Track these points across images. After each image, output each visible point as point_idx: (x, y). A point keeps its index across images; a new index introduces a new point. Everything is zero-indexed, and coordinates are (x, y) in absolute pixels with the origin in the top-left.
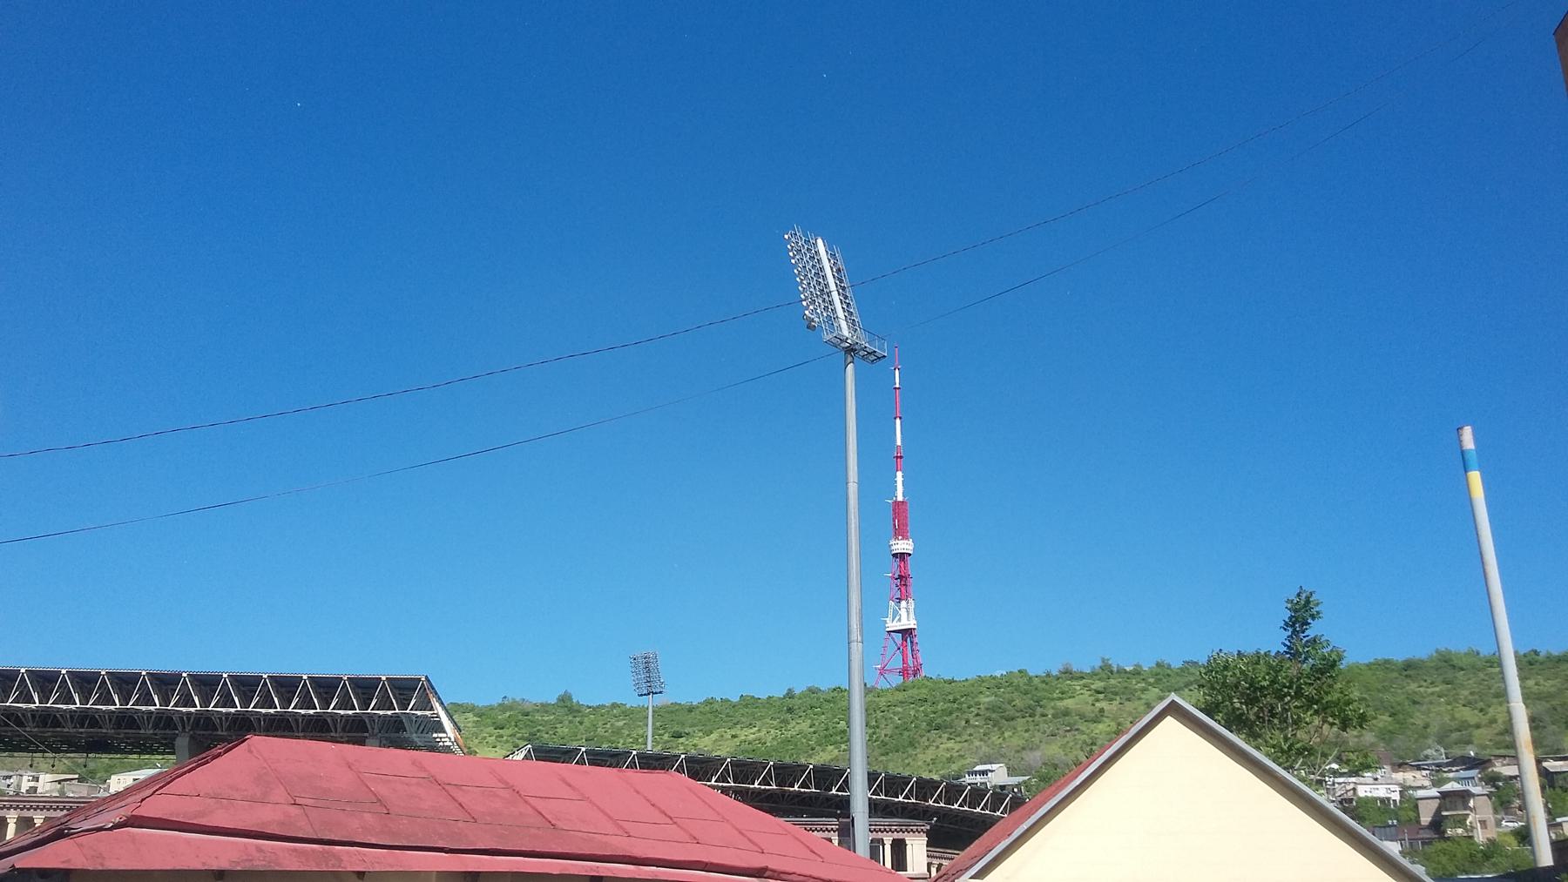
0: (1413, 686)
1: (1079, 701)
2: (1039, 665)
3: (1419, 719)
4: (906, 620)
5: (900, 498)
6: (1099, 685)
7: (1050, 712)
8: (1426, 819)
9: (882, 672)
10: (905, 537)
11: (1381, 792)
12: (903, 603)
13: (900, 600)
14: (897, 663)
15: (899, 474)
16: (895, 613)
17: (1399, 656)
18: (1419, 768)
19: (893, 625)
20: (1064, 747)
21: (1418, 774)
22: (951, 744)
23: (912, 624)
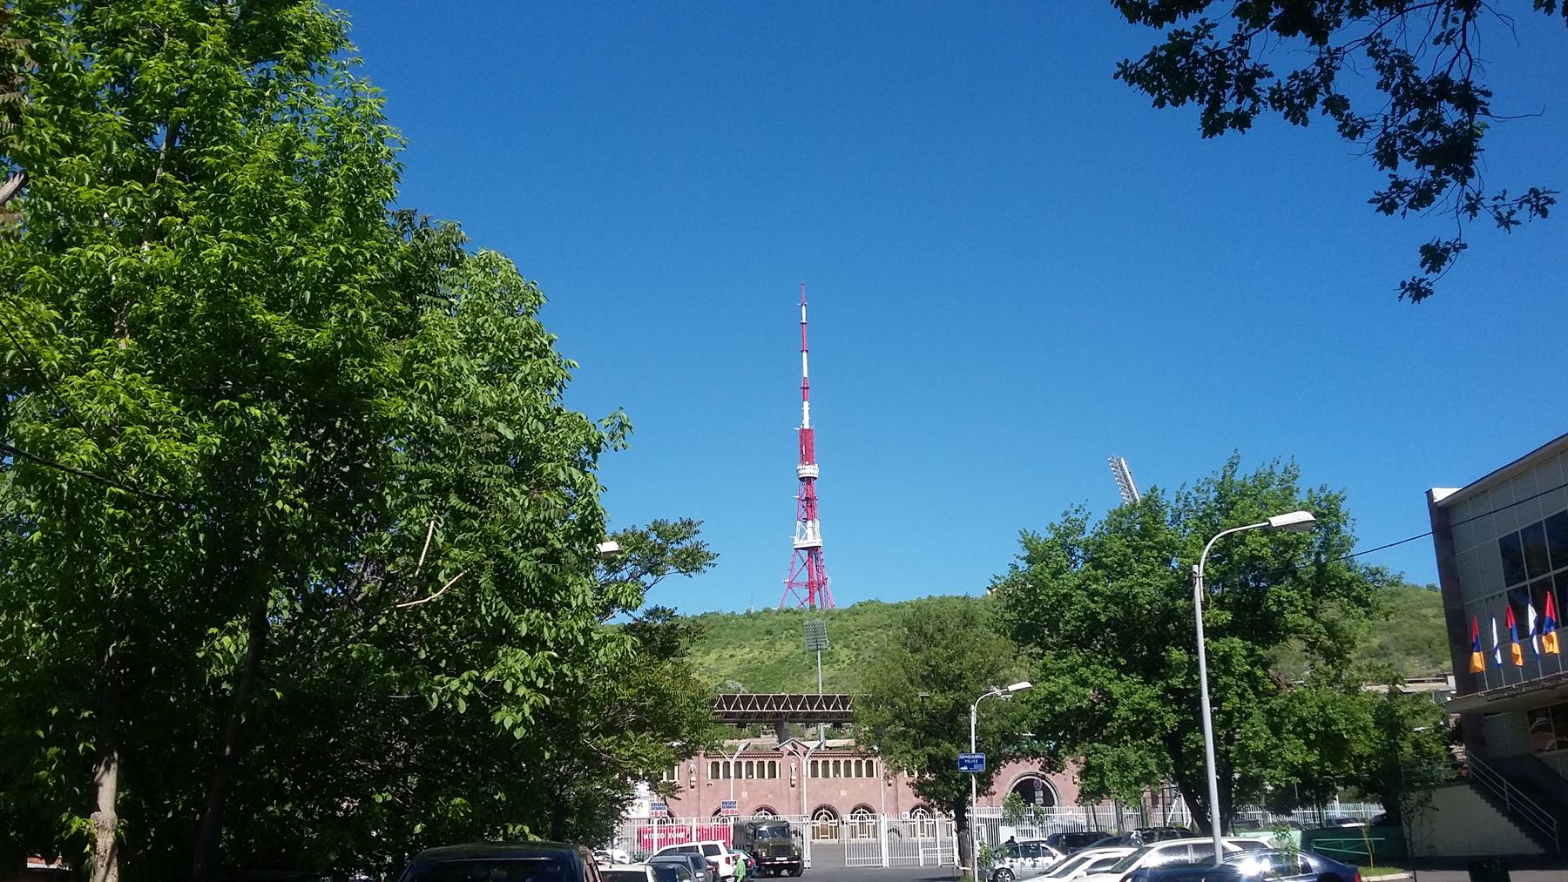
4: (813, 540)
12: (810, 523)
14: (804, 577)
15: (806, 404)
16: (803, 532)
19: (800, 543)
23: (817, 542)
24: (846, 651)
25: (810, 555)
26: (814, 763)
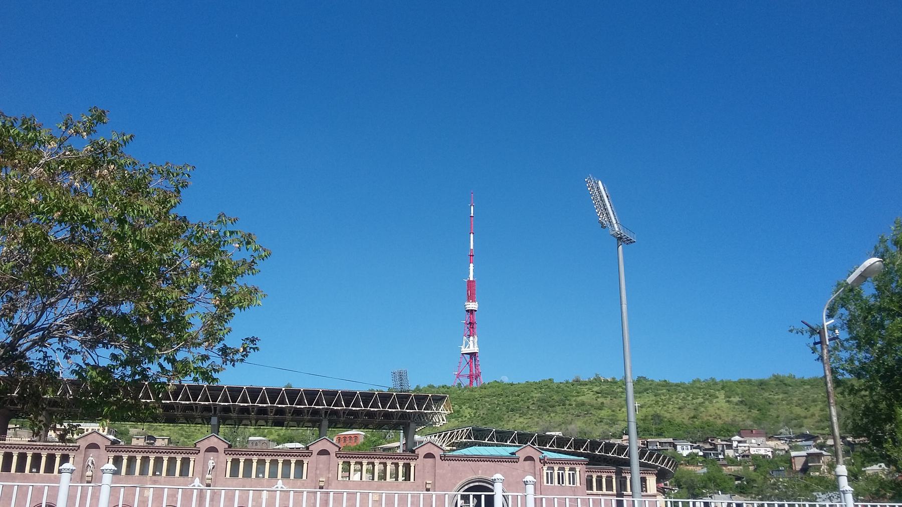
0: (766, 394)
1: (588, 397)
2: (560, 376)
3: (774, 413)
4: (473, 348)
5: (471, 279)
6: (596, 389)
7: (574, 403)
8: (798, 466)
9: (458, 376)
10: (474, 301)
11: (762, 452)
12: (471, 338)
13: (469, 336)
14: (467, 371)
15: (472, 265)
16: (467, 343)
17: (755, 376)
18: (779, 439)
20: (585, 423)
21: (779, 442)
22: (521, 420)
23: (476, 350)
24: (469, 410)
25: (471, 358)
26: (235, 462)
